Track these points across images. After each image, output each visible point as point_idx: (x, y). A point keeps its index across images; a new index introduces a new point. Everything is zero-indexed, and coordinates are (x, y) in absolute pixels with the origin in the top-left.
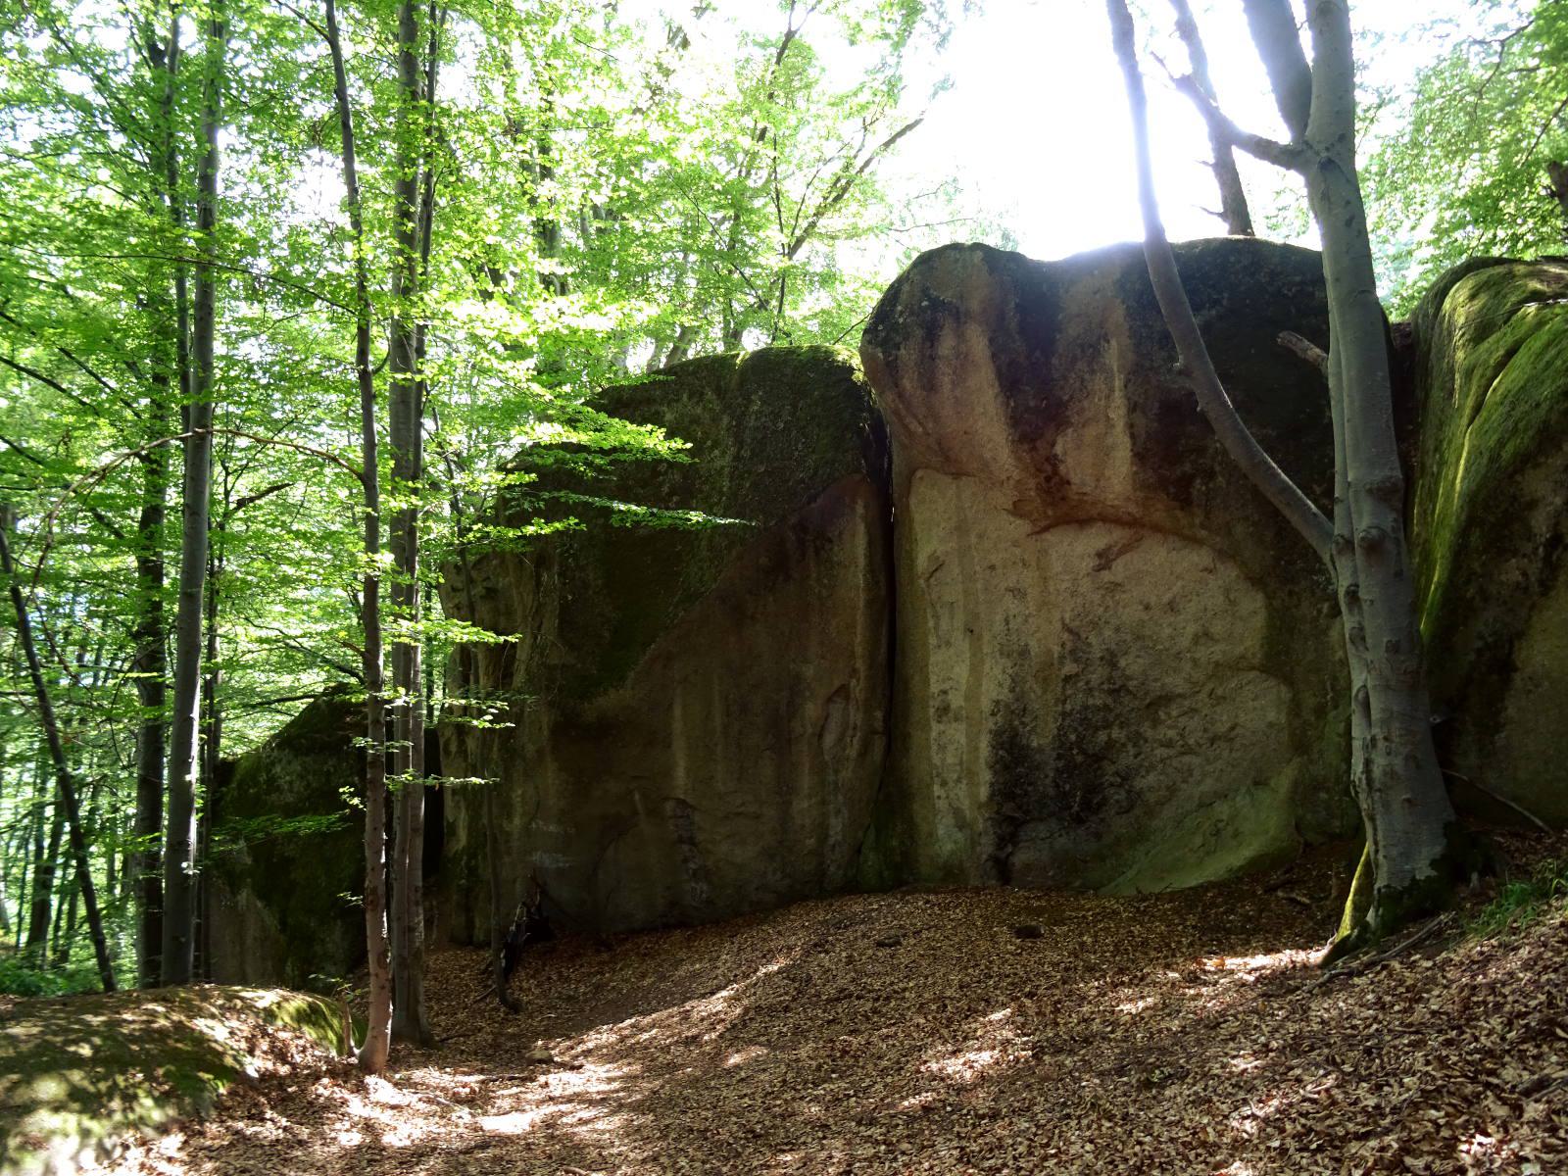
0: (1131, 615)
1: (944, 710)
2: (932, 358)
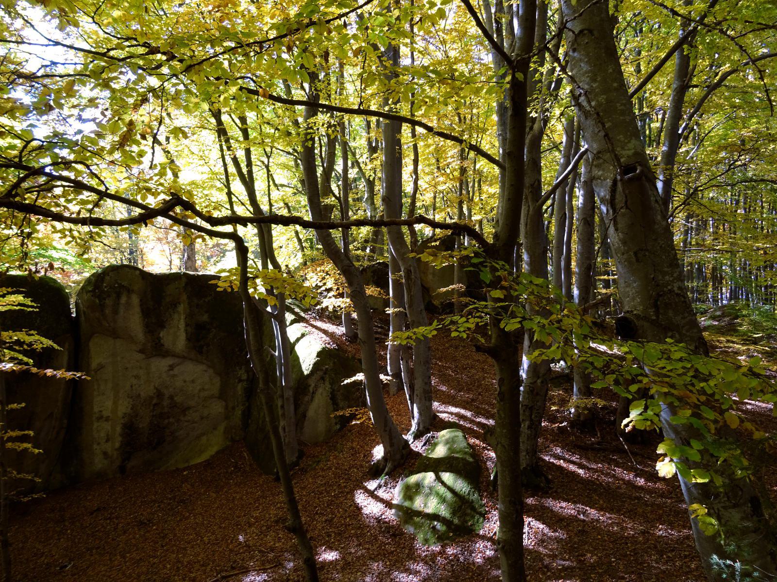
1: (100, 418)
2: (118, 304)
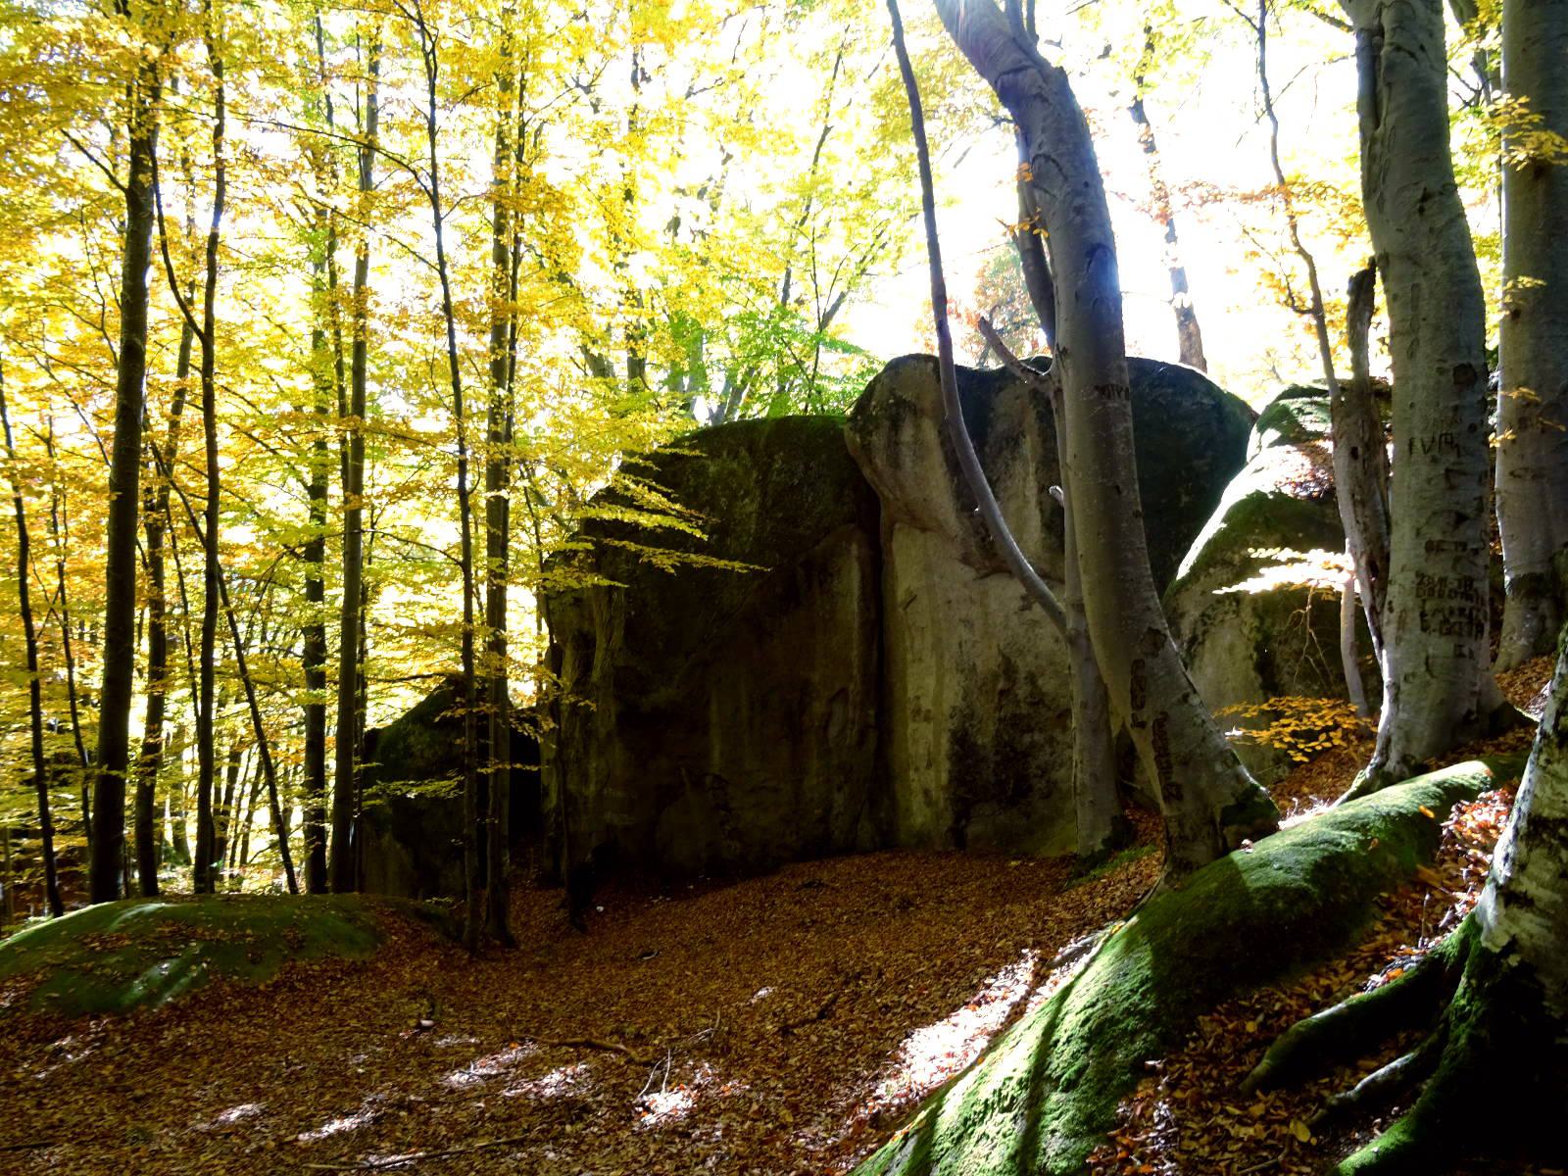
1: (917, 711)
2: (897, 444)
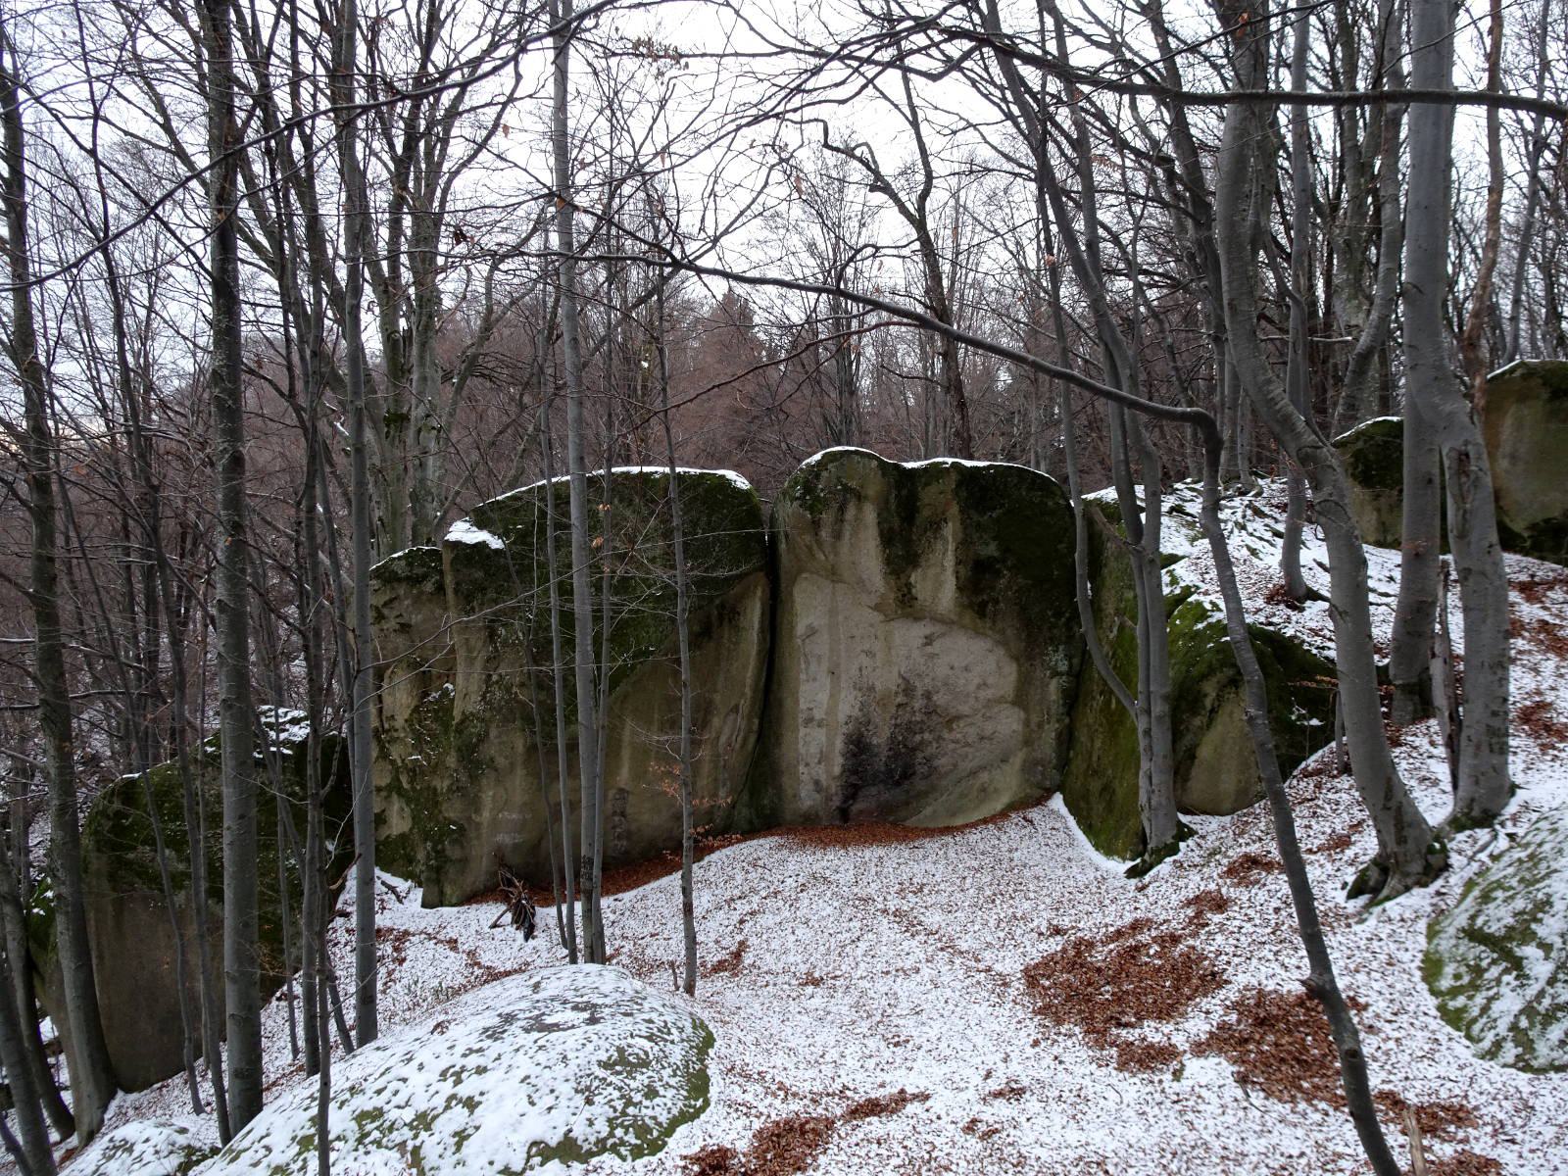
0: (942, 671)
1: (809, 721)
2: (842, 521)
